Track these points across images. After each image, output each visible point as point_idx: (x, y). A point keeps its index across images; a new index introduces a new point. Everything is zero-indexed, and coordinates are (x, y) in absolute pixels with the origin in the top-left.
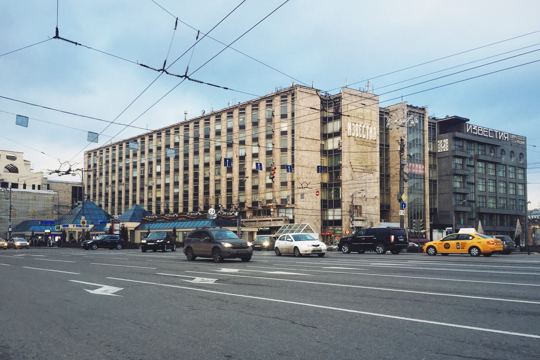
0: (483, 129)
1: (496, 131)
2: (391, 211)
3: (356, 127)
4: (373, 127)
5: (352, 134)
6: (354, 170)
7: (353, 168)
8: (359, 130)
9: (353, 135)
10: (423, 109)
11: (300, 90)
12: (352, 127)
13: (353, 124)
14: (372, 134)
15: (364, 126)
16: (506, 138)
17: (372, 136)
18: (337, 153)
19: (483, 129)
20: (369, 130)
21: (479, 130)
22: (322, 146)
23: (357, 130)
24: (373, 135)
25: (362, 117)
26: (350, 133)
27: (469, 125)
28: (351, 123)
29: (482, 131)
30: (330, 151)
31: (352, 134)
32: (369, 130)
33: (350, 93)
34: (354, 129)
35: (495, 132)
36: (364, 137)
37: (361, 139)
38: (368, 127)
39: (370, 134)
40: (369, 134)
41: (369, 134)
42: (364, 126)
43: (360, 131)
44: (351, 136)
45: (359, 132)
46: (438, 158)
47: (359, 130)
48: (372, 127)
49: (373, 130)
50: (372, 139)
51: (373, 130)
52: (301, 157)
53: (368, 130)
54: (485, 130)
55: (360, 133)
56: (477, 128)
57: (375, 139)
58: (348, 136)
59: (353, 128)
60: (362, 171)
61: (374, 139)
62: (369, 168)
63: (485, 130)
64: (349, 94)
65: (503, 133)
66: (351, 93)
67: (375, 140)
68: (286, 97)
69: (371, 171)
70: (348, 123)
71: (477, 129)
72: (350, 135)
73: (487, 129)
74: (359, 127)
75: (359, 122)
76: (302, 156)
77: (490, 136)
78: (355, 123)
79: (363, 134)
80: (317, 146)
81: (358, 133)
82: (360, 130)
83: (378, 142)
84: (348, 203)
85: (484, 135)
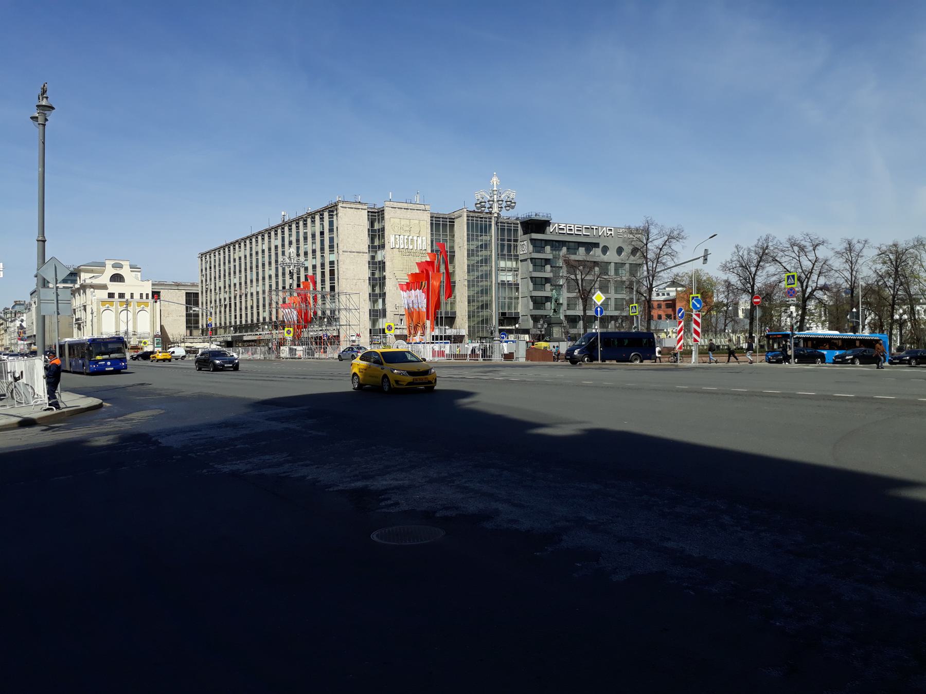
0: (574, 227)
1: (594, 227)
2: (457, 317)
4: (422, 237)
5: (395, 246)
8: (404, 241)
9: (397, 246)
11: (343, 206)
12: (396, 239)
13: (397, 237)
15: (410, 237)
16: (609, 233)
18: (382, 266)
19: (574, 227)
20: (417, 241)
21: (568, 228)
22: (373, 257)
23: (401, 241)
25: (408, 229)
28: (393, 236)
29: (573, 229)
30: (379, 262)
31: (395, 246)
32: (417, 241)
33: (392, 206)
34: (398, 242)
35: (593, 228)
36: (411, 247)
38: (415, 238)
40: (417, 244)
41: (417, 244)
42: (410, 237)
45: (404, 244)
46: (521, 260)
47: (404, 241)
48: (421, 238)
49: (422, 239)
51: (422, 239)
52: (344, 270)
53: (415, 241)
54: (577, 227)
56: (566, 226)
57: (425, 249)
59: (397, 240)
63: (577, 227)
64: (392, 207)
65: (605, 228)
66: (395, 206)
68: (333, 211)
70: (391, 235)
71: (565, 228)
72: (394, 247)
73: (581, 226)
75: (405, 234)
76: (347, 269)
77: (584, 233)
78: (400, 235)
80: (367, 258)
82: (406, 241)
84: (392, 312)
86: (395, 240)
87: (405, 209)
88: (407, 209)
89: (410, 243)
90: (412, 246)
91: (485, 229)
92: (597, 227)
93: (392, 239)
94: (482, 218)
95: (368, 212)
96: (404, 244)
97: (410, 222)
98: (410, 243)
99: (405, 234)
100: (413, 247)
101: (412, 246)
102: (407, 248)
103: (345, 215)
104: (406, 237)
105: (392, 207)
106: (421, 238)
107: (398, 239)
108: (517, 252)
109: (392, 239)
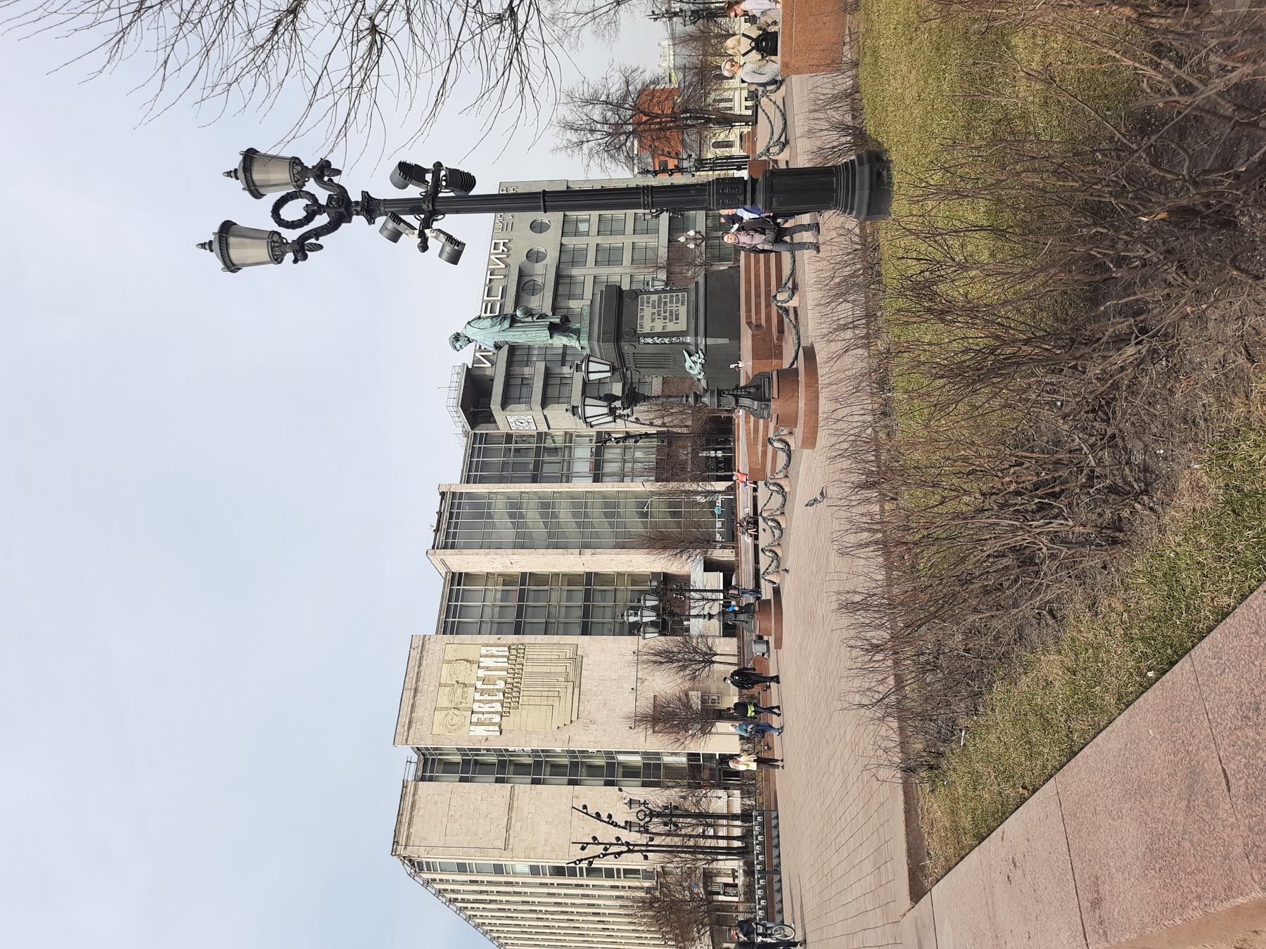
1: (489, 277)
3: (481, 710)
5: (495, 724)
6: (574, 718)
7: (571, 721)
9: (497, 718)
10: (443, 494)
12: (479, 723)
14: (495, 659)
15: (479, 685)
16: (501, 247)
17: (499, 660)
20: (488, 668)
23: (486, 708)
24: (498, 656)
25: (460, 691)
26: (491, 728)
27: (477, 361)
28: (472, 728)
31: (495, 724)
34: (486, 716)
36: (501, 685)
37: (506, 695)
38: (481, 673)
39: (495, 665)
40: (496, 669)
42: (479, 685)
43: (490, 698)
44: (500, 727)
45: (492, 701)
48: (481, 659)
50: (506, 660)
51: (486, 656)
53: (488, 673)
55: (494, 698)
57: (506, 649)
58: (499, 733)
60: (577, 690)
61: (507, 654)
62: (571, 670)
64: (409, 728)
65: (492, 257)
67: (510, 648)
69: (577, 661)
70: (471, 733)
72: (497, 728)
73: (484, 304)
74: (479, 701)
75: (470, 699)
77: (499, 298)
79: (496, 687)
81: (493, 705)
82: (486, 697)
83: (513, 639)
85: (497, 313)
86: (483, 724)
87: (415, 696)
88: (416, 690)
89: (492, 687)
90: (498, 682)
91: (482, 508)
92: (489, 272)
93: (480, 731)
94: (451, 514)
95: (423, 779)
96: (492, 701)
97: (446, 685)
98: (492, 687)
99: (470, 699)
100: (500, 679)
101: (498, 682)
102: (501, 694)
103: (425, 839)
104: (478, 696)
105: (409, 728)
106: (481, 659)
107: (481, 716)
108: (533, 436)
109: (480, 731)
